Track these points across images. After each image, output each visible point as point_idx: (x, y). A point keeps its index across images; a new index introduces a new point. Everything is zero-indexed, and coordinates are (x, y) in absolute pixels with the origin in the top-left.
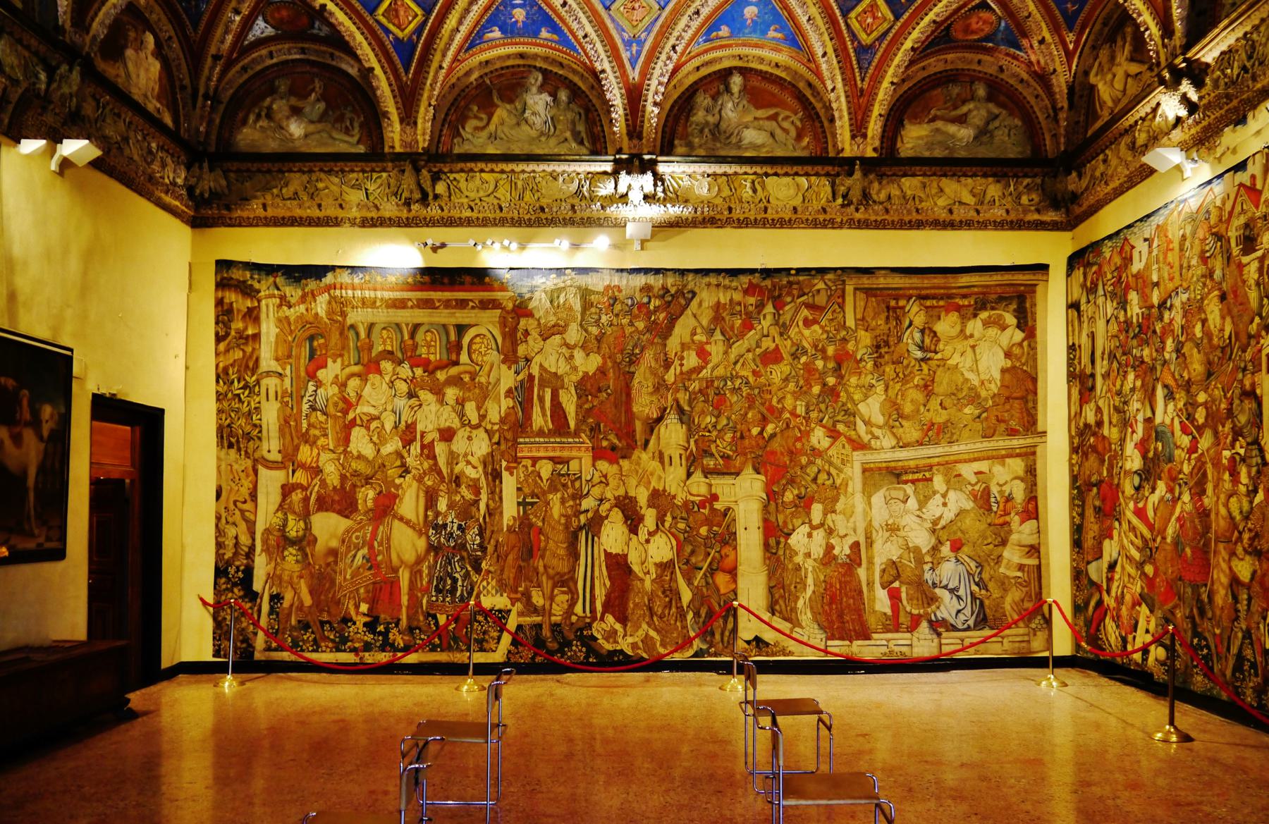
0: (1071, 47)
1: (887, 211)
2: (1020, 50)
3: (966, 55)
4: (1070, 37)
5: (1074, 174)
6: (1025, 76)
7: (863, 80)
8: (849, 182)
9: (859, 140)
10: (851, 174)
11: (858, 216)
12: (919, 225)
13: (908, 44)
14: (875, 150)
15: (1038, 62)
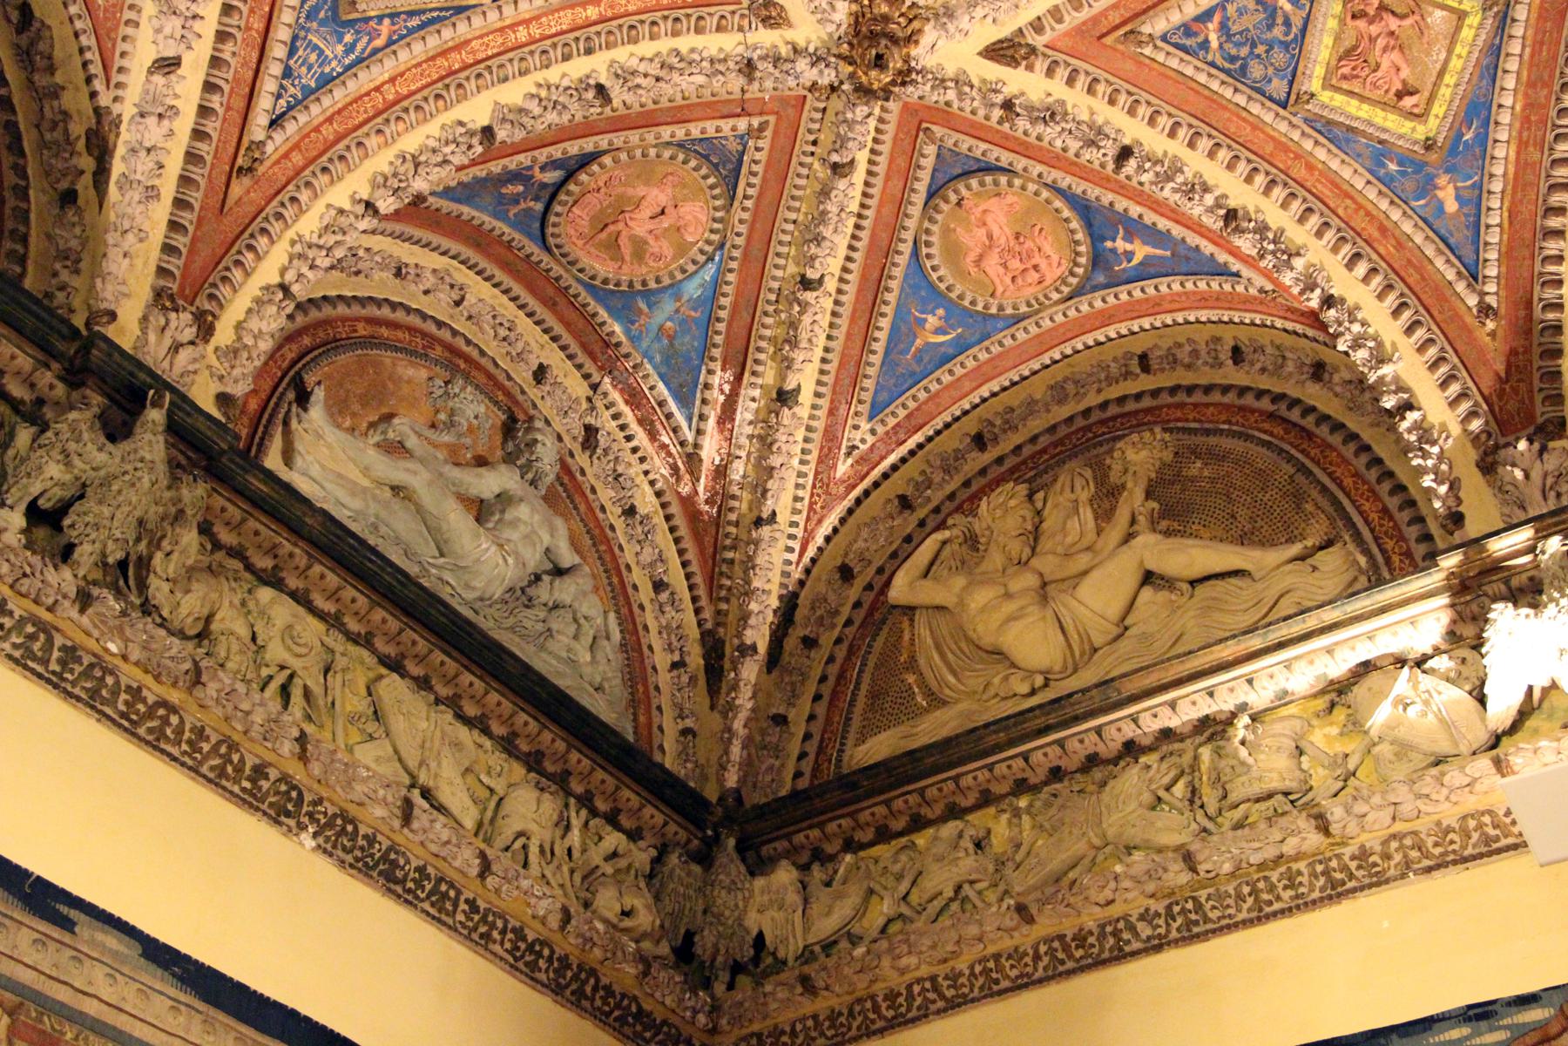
0: (843, 468)
1: (196, 678)
2: (685, 401)
3: (524, 323)
4: (861, 434)
5: (785, 875)
6: (646, 502)
7: (275, 123)
8: (96, 455)
9: (182, 325)
10: (117, 429)
11: (72, 624)
12: (282, 805)
13: (477, 110)
14: (223, 399)
15: (721, 472)
